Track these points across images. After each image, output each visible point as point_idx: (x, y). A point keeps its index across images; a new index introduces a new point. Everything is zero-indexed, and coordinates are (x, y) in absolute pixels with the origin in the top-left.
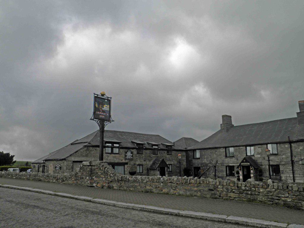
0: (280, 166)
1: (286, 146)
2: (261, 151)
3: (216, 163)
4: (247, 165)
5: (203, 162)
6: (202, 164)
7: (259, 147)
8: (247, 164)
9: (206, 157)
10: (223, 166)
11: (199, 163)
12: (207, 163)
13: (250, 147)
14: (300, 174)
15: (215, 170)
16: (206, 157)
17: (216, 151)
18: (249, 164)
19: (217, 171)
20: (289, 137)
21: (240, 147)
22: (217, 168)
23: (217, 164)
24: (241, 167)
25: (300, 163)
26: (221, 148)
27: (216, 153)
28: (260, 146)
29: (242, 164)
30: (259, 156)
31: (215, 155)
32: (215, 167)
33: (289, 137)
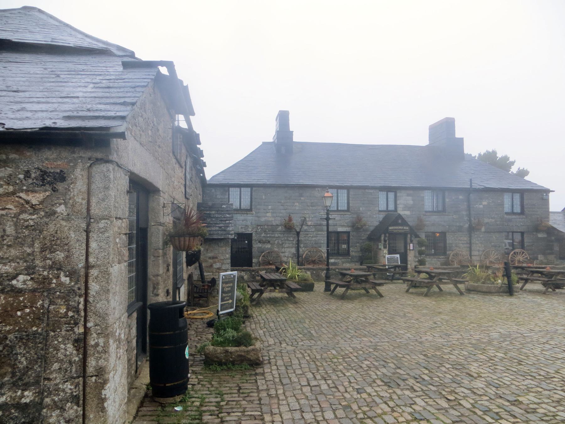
0: (448, 235)
1: (461, 197)
2: (411, 202)
3: (302, 226)
4: (403, 231)
5: (263, 219)
6: (258, 226)
7: (408, 195)
8: (403, 229)
9: (270, 207)
10: (319, 233)
11: (249, 223)
12: (274, 224)
13: (386, 192)
14: (479, 251)
15: (298, 240)
16: (270, 207)
17: (301, 195)
18: (407, 228)
19: (302, 245)
20: (471, 180)
21: (367, 191)
22: (302, 237)
23: (305, 228)
24: (387, 235)
25: (482, 231)
26: (317, 189)
27: (302, 198)
28: (411, 192)
29: (390, 228)
30: (408, 213)
31: (297, 204)
32: (298, 234)
33: (471, 180)
